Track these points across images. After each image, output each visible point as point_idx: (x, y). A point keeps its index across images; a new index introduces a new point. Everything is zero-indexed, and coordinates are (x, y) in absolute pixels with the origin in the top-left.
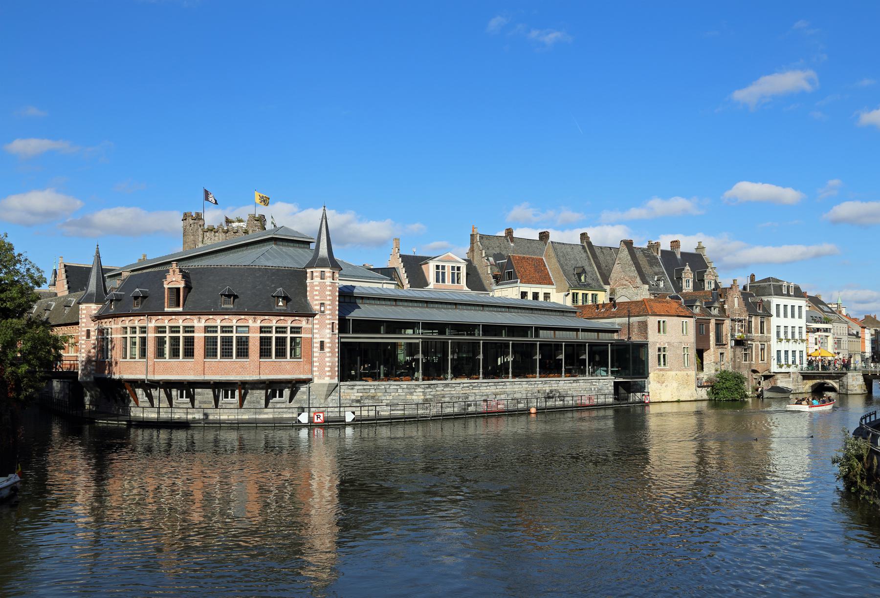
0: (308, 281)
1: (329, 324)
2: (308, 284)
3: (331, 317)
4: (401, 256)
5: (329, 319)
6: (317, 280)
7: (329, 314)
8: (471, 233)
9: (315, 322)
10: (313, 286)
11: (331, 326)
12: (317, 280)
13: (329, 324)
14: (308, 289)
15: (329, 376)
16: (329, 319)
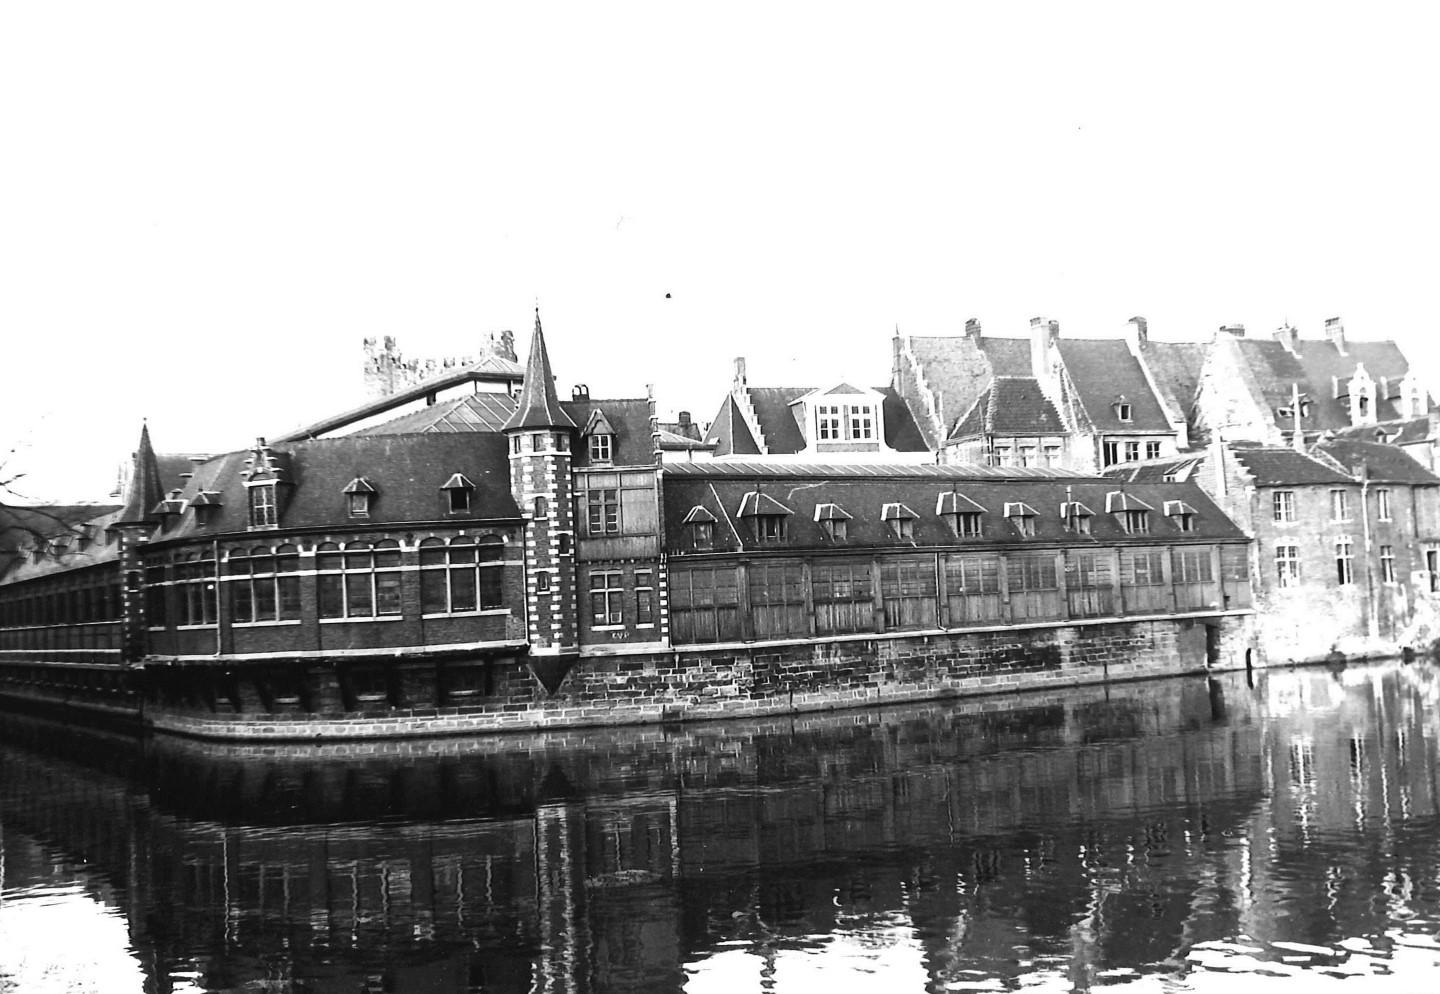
0: (512, 455)
1: (556, 538)
2: (512, 462)
3: (557, 524)
4: (748, 390)
5: (556, 528)
6: (527, 451)
7: (555, 519)
8: (895, 336)
9: (529, 534)
10: (519, 468)
11: (557, 542)
12: (527, 451)
13: (556, 538)
14: (513, 471)
15: (560, 640)
16: (556, 528)
